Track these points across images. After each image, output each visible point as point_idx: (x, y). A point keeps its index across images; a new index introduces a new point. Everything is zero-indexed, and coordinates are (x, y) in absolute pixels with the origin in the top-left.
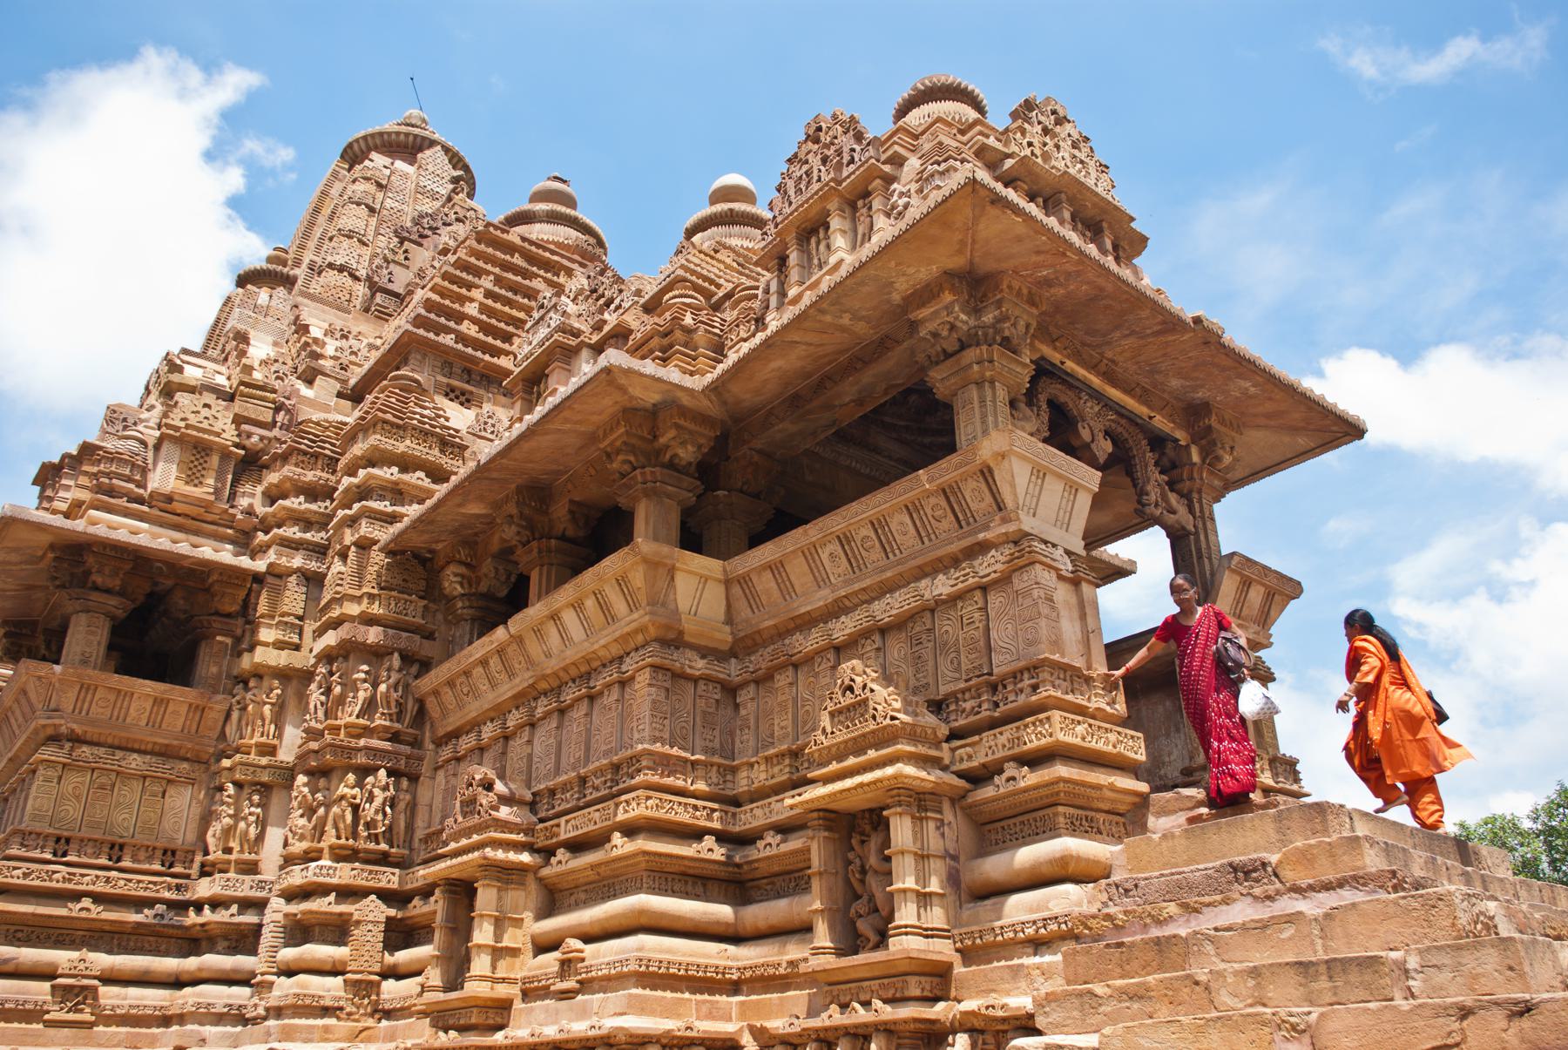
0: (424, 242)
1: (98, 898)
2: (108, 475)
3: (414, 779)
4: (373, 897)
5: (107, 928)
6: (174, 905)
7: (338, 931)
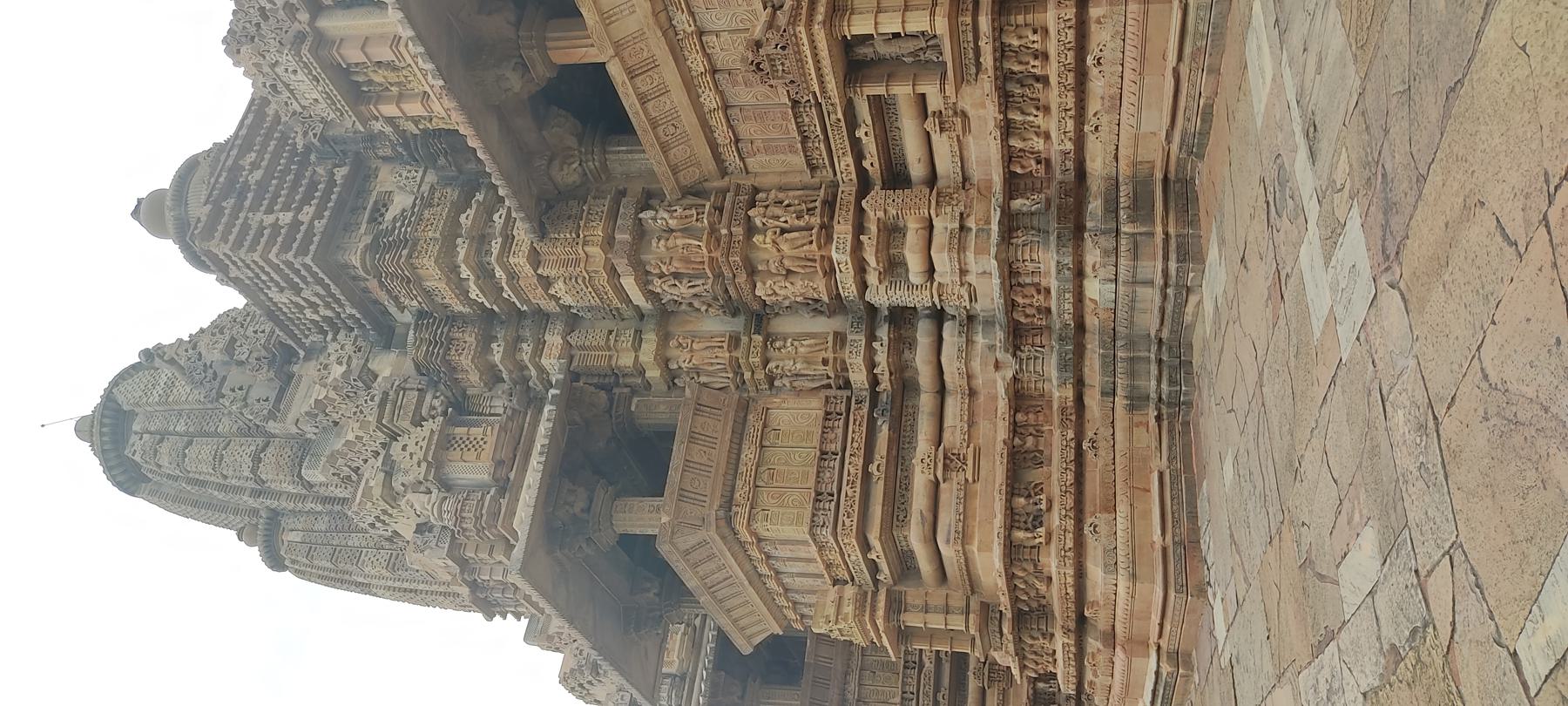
0: (221, 374)
1: (868, 459)
2: (478, 518)
3: (756, 190)
4: (864, 203)
5: (894, 452)
6: (874, 404)
7: (892, 232)
